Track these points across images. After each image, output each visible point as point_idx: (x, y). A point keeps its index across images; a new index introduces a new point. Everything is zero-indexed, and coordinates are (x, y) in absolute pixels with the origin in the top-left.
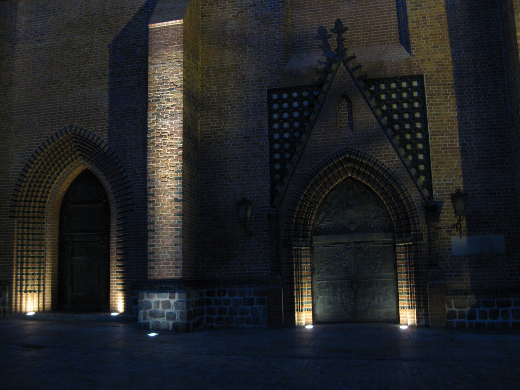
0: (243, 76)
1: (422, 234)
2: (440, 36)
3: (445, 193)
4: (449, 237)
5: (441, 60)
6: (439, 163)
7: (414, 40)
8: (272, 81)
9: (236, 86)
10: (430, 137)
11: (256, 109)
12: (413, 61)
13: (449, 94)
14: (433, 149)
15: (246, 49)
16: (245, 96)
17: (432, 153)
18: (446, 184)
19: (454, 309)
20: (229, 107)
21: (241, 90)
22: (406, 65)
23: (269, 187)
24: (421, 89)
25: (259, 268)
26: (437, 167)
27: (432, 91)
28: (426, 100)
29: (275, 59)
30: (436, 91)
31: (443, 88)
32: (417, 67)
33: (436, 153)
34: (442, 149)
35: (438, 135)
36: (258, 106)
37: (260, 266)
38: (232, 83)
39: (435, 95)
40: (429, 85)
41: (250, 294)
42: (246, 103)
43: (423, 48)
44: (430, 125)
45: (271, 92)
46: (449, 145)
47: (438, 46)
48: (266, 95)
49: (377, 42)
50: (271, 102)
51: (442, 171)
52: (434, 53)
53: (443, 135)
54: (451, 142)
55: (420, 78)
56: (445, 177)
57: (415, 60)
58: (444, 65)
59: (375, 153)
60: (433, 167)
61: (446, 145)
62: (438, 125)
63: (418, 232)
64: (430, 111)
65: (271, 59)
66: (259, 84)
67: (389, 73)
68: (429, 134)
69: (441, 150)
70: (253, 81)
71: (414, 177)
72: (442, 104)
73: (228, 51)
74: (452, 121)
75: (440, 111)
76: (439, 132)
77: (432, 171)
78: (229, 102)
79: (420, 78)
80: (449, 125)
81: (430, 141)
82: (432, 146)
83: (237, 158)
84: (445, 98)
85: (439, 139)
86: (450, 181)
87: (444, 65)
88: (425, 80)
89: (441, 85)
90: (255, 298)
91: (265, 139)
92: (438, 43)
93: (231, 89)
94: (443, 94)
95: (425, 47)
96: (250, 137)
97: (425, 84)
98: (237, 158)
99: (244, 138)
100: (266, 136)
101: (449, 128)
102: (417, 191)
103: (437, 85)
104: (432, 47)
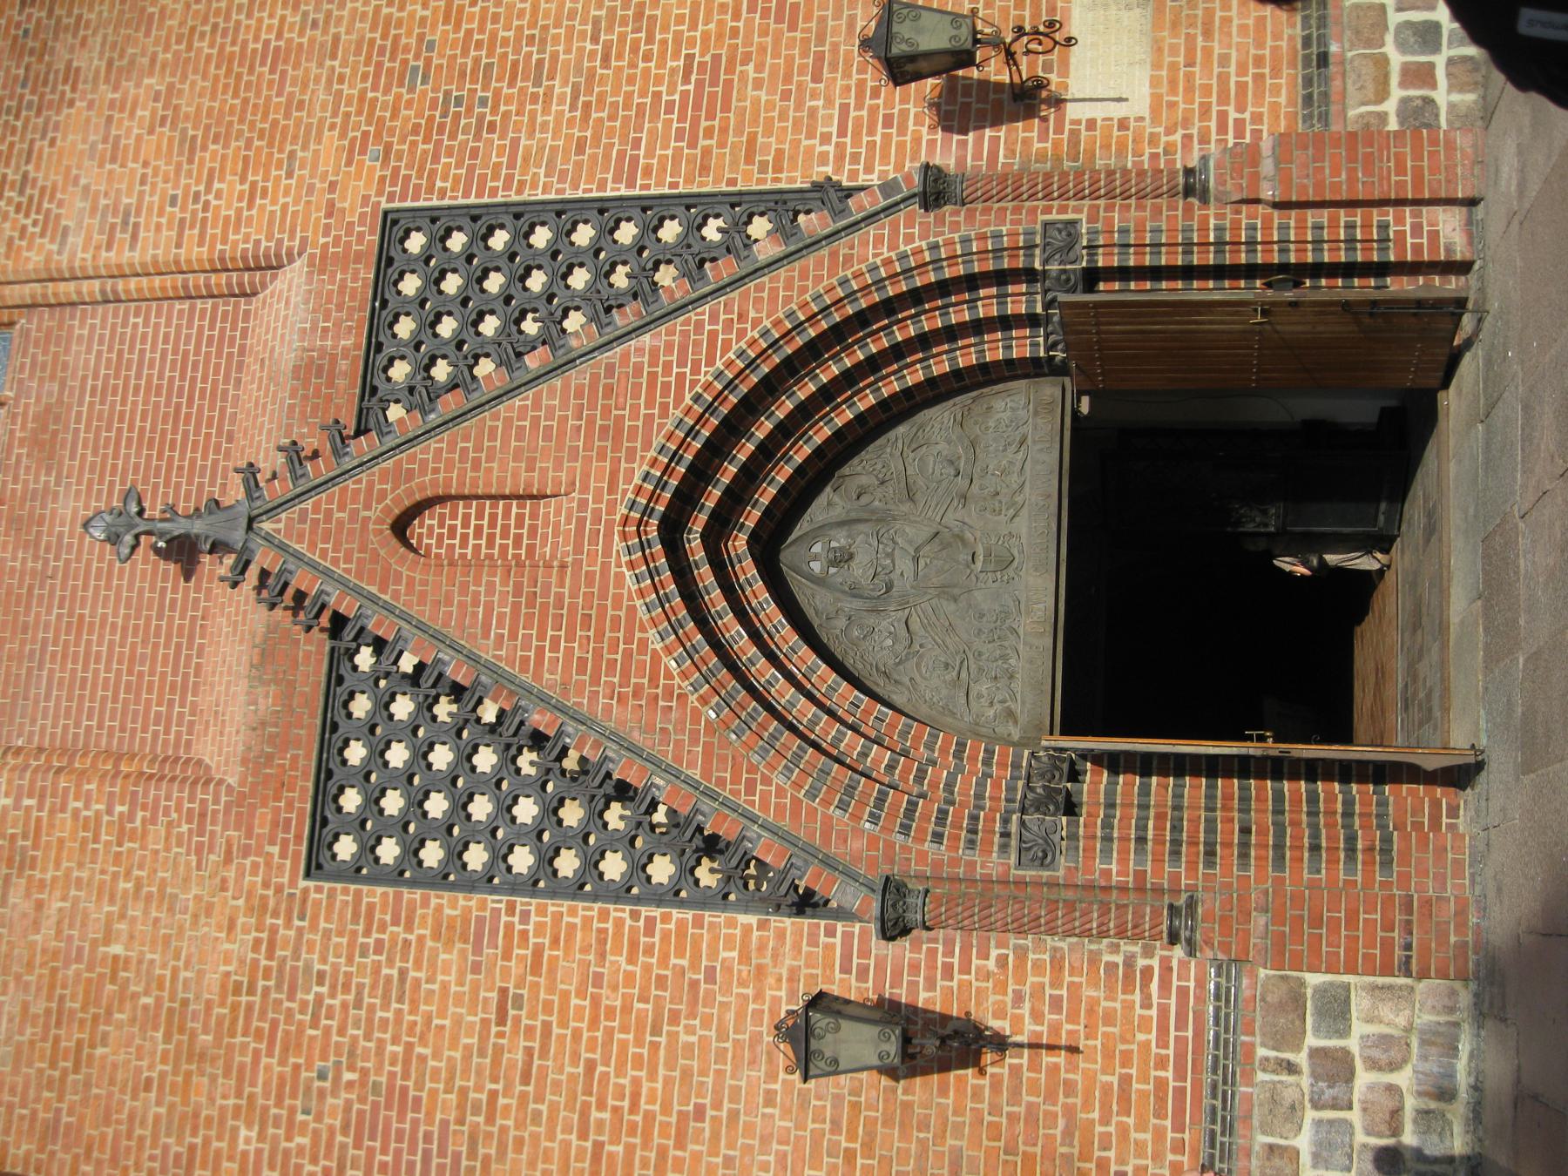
0: (223, 986)
1: (1046, 225)
2: (257, 143)
3: (878, 138)
4: (1067, 127)
5: (346, 143)
6: (749, 160)
7: (246, 241)
8: (275, 850)
9: (259, 1032)
10: (637, 192)
11: (379, 942)
12: (326, 245)
13: (481, 117)
14: (686, 182)
15: (116, 958)
16: (316, 989)
17: (701, 184)
18: (842, 133)
19: (1390, 106)
20: (348, 1076)
21: (287, 1004)
22: (333, 275)
23: (752, 919)
24: (439, 222)
25: (1154, 1012)
26: (763, 167)
27: (457, 179)
28: (486, 200)
29: (185, 828)
30: (459, 165)
31: (453, 136)
32: (349, 233)
33: (705, 169)
34: (692, 144)
35: (635, 160)
36: (367, 933)
37: (1146, 1005)
38: (244, 1046)
39: (471, 169)
40: (430, 190)
41: (1291, 1068)
42: (346, 988)
43: (285, 207)
44: (591, 190)
45: (317, 863)
46: (681, 119)
47: (292, 154)
48: (326, 885)
49: (225, 392)
50: (364, 869)
51: (787, 146)
52: (315, 166)
53: (636, 143)
54: (669, 111)
55: (395, 222)
56: (811, 136)
57: (322, 240)
58: (366, 134)
59: (664, 408)
60: (764, 181)
61: (681, 132)
62: (594, 157)
63: (1038, 240)
64: (534, 186)
65: (179, 845)
66: (275, 914)
67: (351, 342)
68: (624, 192)
69: (699, 151)
70: (258, 942)
71: (792, 248)
72: (515, 143)
73: (105, 1045)
74: (587, 105)
75: (541, 149)
76: (622, 154)
77: (783, 186)
78: (322, 1076)
79: (393, 226)
80: (601, 120)
81: (653, 191)
82: (674, 185)
83: (591, 1066)
84: (492, 127)
85: (650, 153)
86: (831, 117)
87: (366, 134)
88: (408, 204)
89: (439, 143)
90: (1311, 1041)
91: (525, 916)
92: (281, 151)
93: (270, 1054)
94: (478, 137)
95: (282, 201)
96: (503, 992)
97: (421, 203)
98: (591, 1066)
99: (501, 1021)
100: (511, 909)
101: (612, 118)
102: (856, 237)
103: (436, 159)
104: (290, 175)
